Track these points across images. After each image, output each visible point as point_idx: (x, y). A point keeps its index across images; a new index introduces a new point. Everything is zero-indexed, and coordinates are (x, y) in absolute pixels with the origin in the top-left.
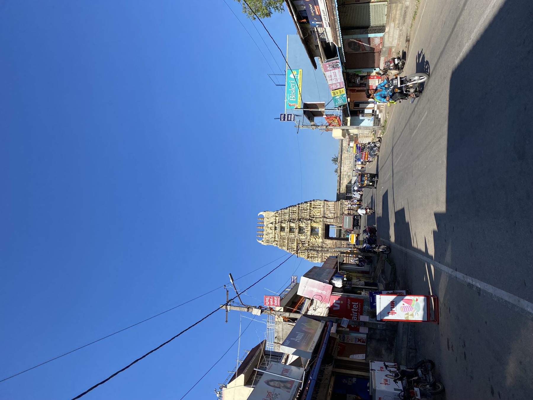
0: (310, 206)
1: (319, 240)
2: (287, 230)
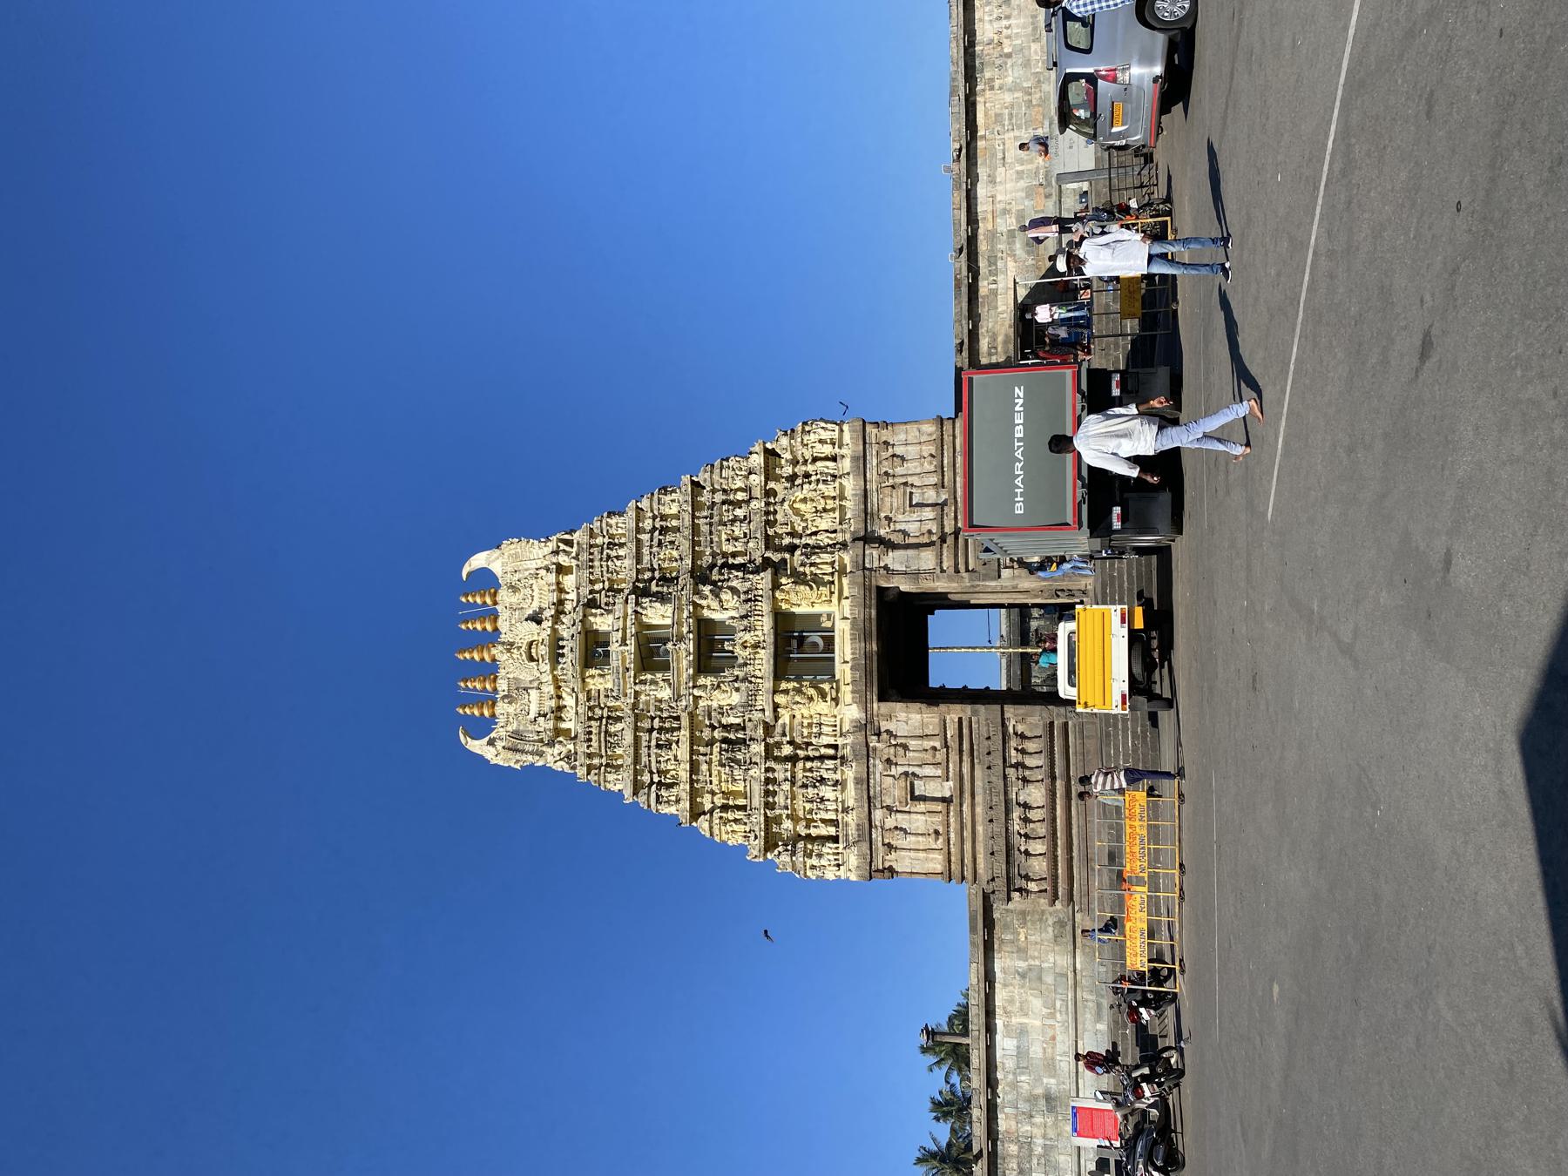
0: (769, 475)
1: (834, 711)
2: (622, 653)
